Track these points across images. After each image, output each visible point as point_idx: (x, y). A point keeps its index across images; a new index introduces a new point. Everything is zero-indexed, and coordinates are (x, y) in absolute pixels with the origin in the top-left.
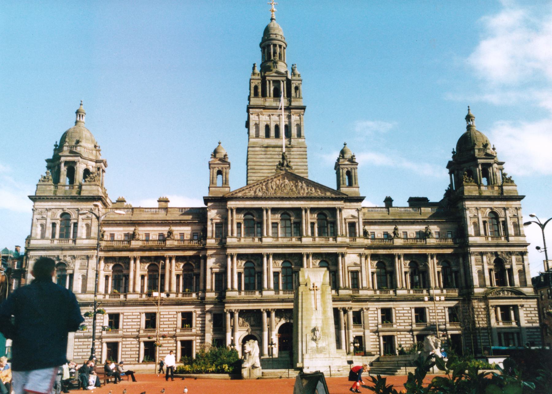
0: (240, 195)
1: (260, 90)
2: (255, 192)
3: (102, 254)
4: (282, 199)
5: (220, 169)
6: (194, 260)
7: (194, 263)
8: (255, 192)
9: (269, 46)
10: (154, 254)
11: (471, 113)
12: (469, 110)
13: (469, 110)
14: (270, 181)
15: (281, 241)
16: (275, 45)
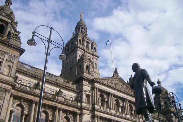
0: (101, 81)
1: (81, 42)
2: (107, 83)
3: (14, 92)
4: (118, 91)
5: (88, 65)
6: (71, 115)
7: (71, 117)
8: (107, 83)
9: (79, 28)
10: (50, 103)
11: (159, 80)
12: (158, 79)
13: (158, 79)
14: (113, 80)
15: (118, 114)
16: (82, 28)
